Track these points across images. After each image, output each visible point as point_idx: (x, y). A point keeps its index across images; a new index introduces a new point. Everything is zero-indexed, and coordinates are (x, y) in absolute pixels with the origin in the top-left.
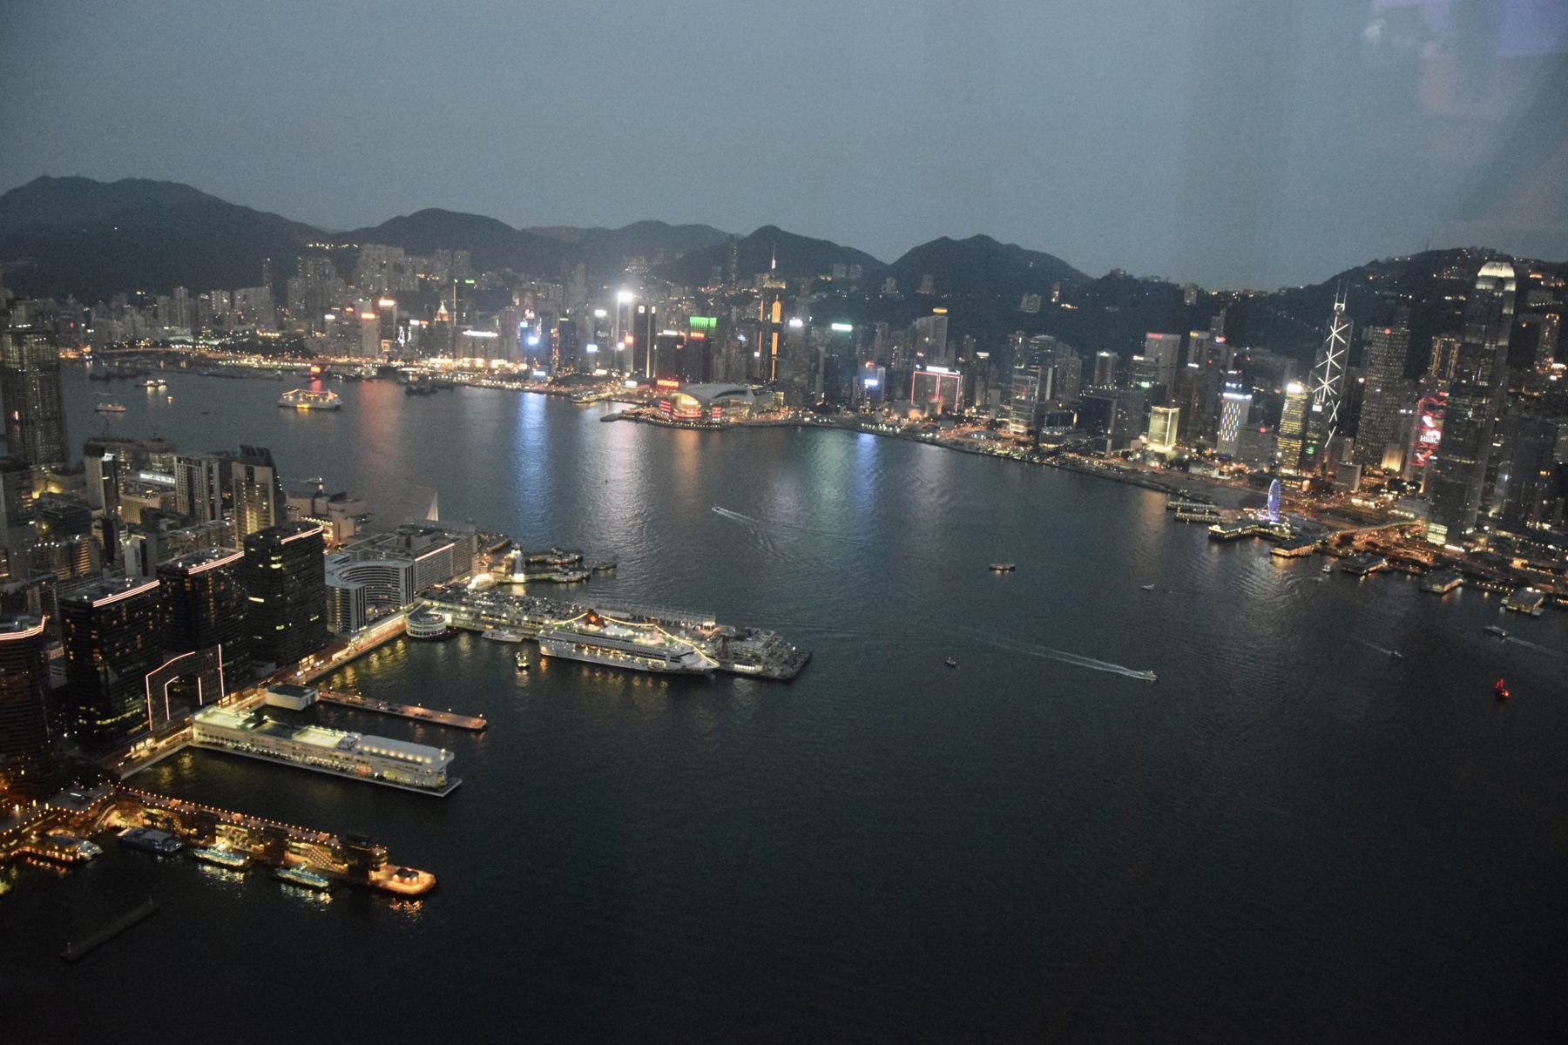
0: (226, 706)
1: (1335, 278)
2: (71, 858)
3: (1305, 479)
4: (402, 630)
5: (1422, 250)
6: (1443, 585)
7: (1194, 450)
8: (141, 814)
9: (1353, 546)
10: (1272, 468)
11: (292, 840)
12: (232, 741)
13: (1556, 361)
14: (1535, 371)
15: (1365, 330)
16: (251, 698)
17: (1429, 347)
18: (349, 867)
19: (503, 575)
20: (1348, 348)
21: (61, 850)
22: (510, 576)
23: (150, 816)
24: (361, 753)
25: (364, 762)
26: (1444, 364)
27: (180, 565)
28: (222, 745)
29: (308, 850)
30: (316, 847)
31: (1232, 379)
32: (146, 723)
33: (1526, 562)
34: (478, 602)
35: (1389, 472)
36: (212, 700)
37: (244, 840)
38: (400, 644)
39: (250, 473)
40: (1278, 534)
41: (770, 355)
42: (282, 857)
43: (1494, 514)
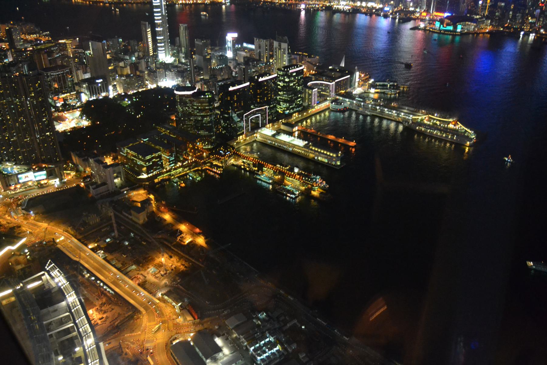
0: (267, 128)
2: (220, 172)
4: (328, 107)
8: (241, 161)
11: (287, 176)
12: (270, 140)
16: (276, 126)
18: (305, 189)
19: (367, 89)
21: (217, 169)
22: (369, 90)
23: (243, 162)
24: (311, 150)
25: (312, 153)
27: (256, 77)
28: (266, 142)
29: (292, 181)
30: (295, 180)
32: (243, 131)
34: (357, 99)
36: (264, 125)
37: (271, 174)
38: (327, 113)
39: (280, 46)
41: (486, 3)
42: (283, 182)
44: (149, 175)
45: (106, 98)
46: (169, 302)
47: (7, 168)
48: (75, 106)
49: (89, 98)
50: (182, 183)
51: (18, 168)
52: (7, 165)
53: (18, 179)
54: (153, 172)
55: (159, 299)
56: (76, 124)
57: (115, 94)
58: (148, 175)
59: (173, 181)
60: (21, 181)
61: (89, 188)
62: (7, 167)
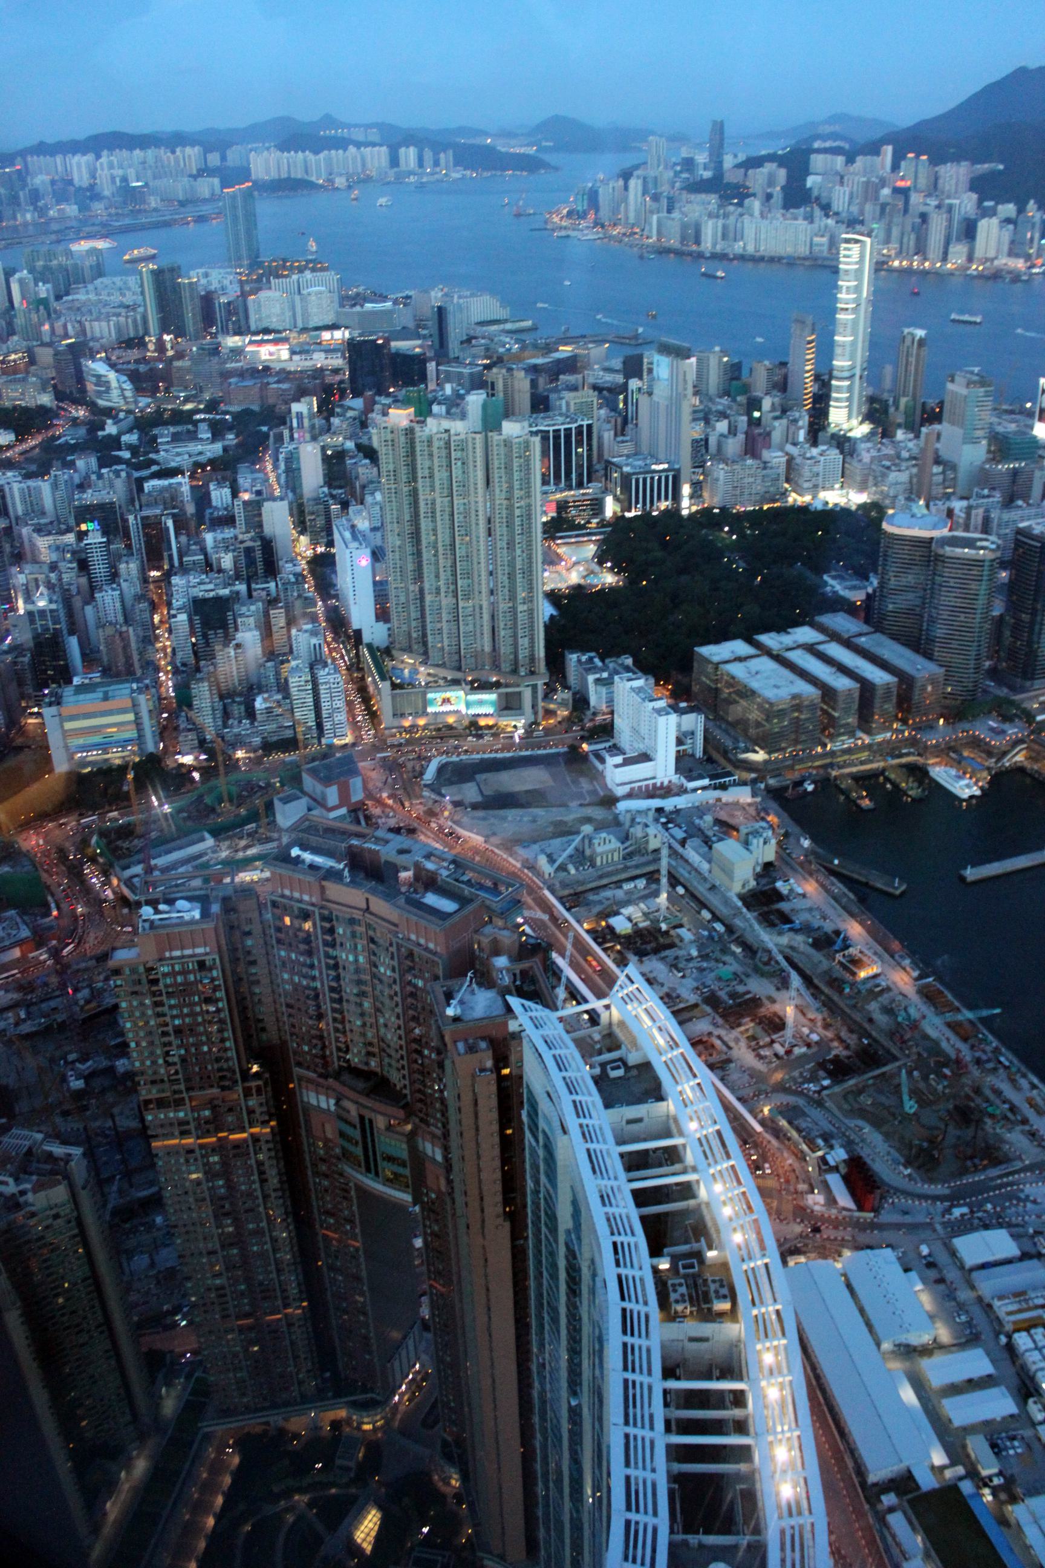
44: (774, 756)
45: (673, 514)
46: (789, 1139)
47: (402, 670)
48: (583, 527)
49: (623, 511)
50: (862, 798)
51: (429, 674)
52: (403, 662)
53: (426, 703)
54: (784, 749)
55: (762, 1123)
56: (584, 577)
57: (694, 508)
58: (769, 753)
59: (837, 787)
60: (430, 710)
61: (602, 761)
62: (401, 666)
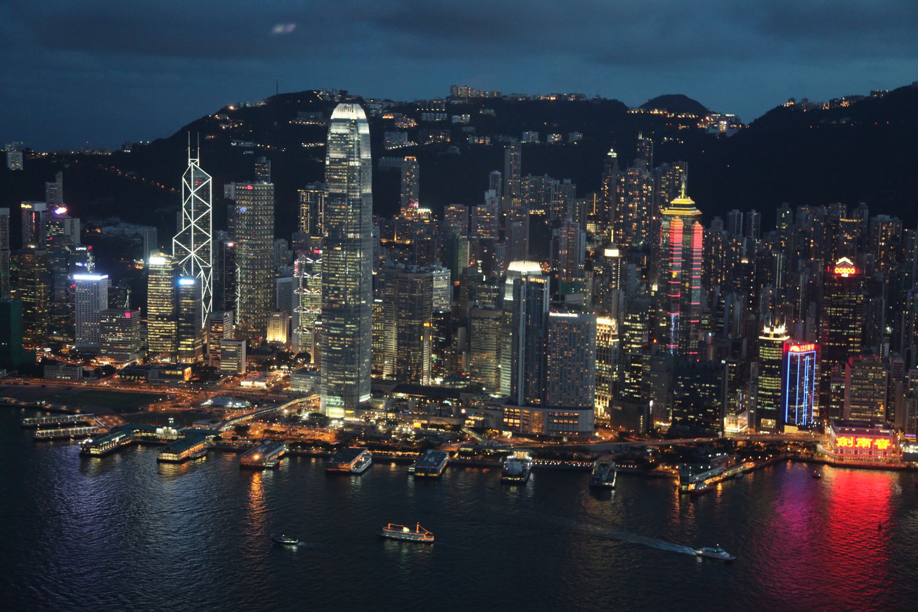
1: (184, 131)
3: (186, 366)
5: (275, 94)
6: (349, 460)
7: (48, 350)
9: (248, 435)
10: (145, 360)
13: (421, 206)
14: (402, 218)
15: (226, 186)
17: (296, 202)
20: (211, 209)
26: (314, 221)
31: (83, 258)
33: (425, 422)
35: (275, 345)
40: (163, 437)
43: (387, 375)
